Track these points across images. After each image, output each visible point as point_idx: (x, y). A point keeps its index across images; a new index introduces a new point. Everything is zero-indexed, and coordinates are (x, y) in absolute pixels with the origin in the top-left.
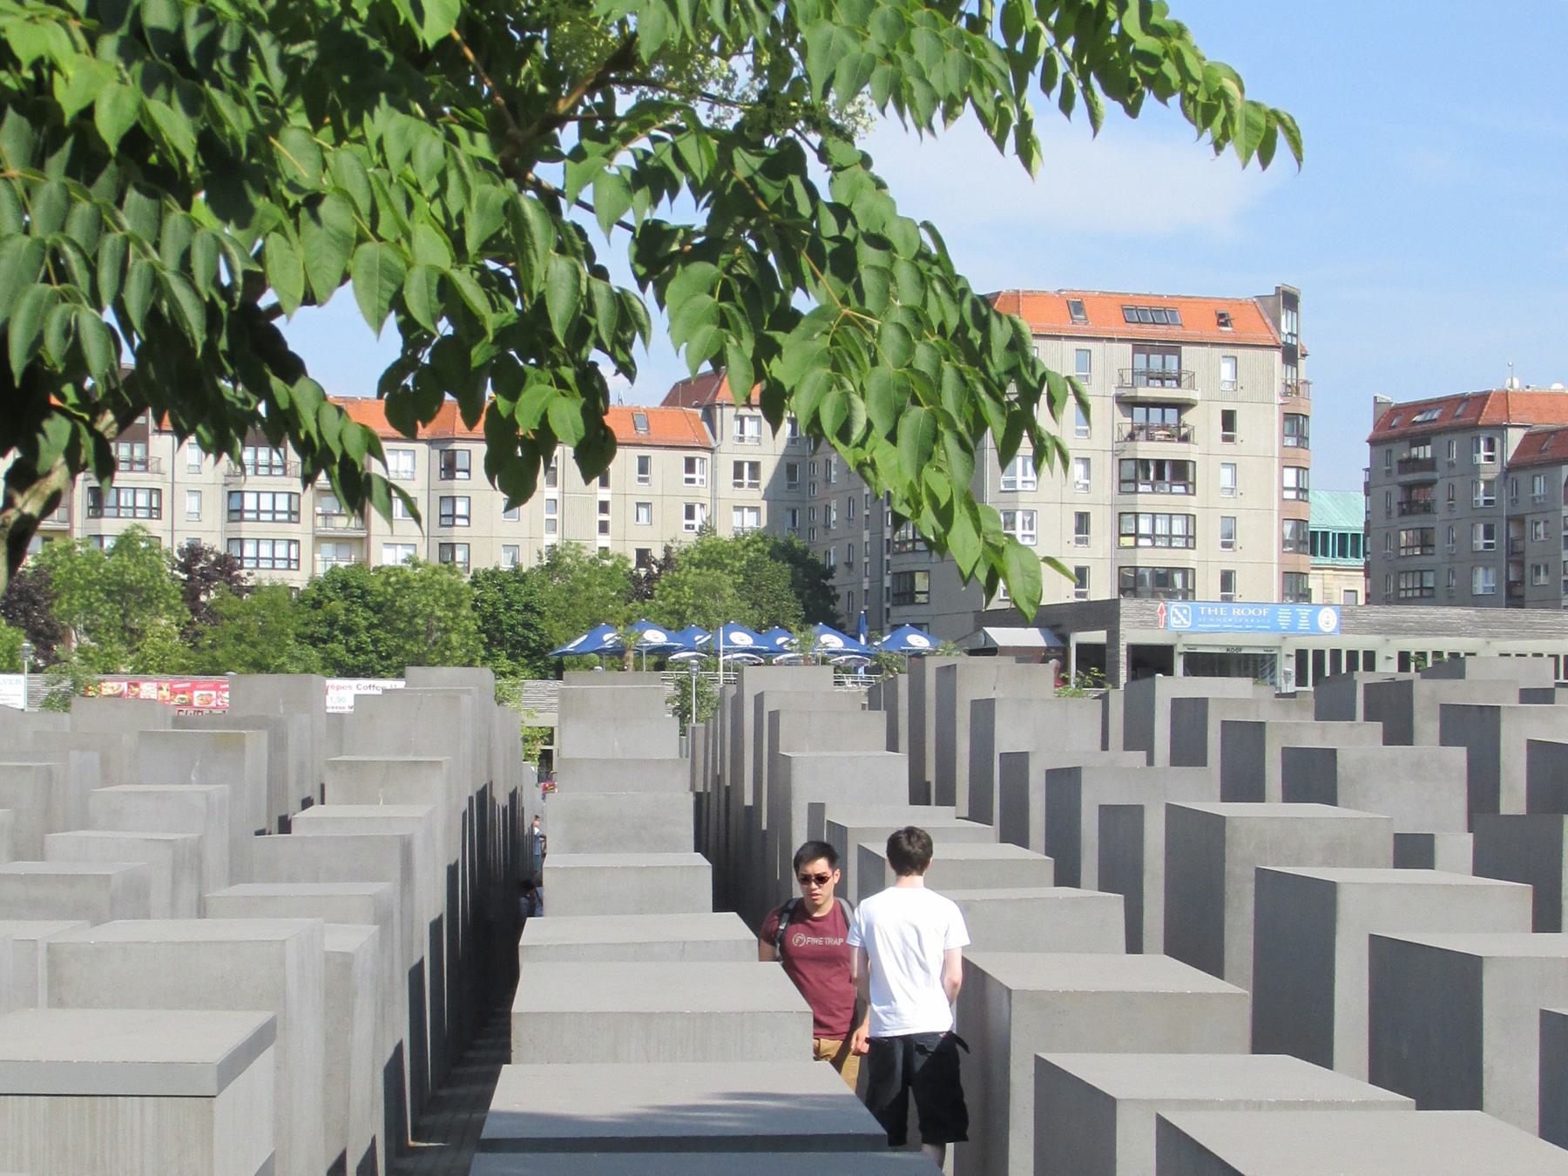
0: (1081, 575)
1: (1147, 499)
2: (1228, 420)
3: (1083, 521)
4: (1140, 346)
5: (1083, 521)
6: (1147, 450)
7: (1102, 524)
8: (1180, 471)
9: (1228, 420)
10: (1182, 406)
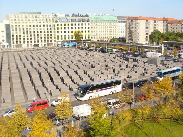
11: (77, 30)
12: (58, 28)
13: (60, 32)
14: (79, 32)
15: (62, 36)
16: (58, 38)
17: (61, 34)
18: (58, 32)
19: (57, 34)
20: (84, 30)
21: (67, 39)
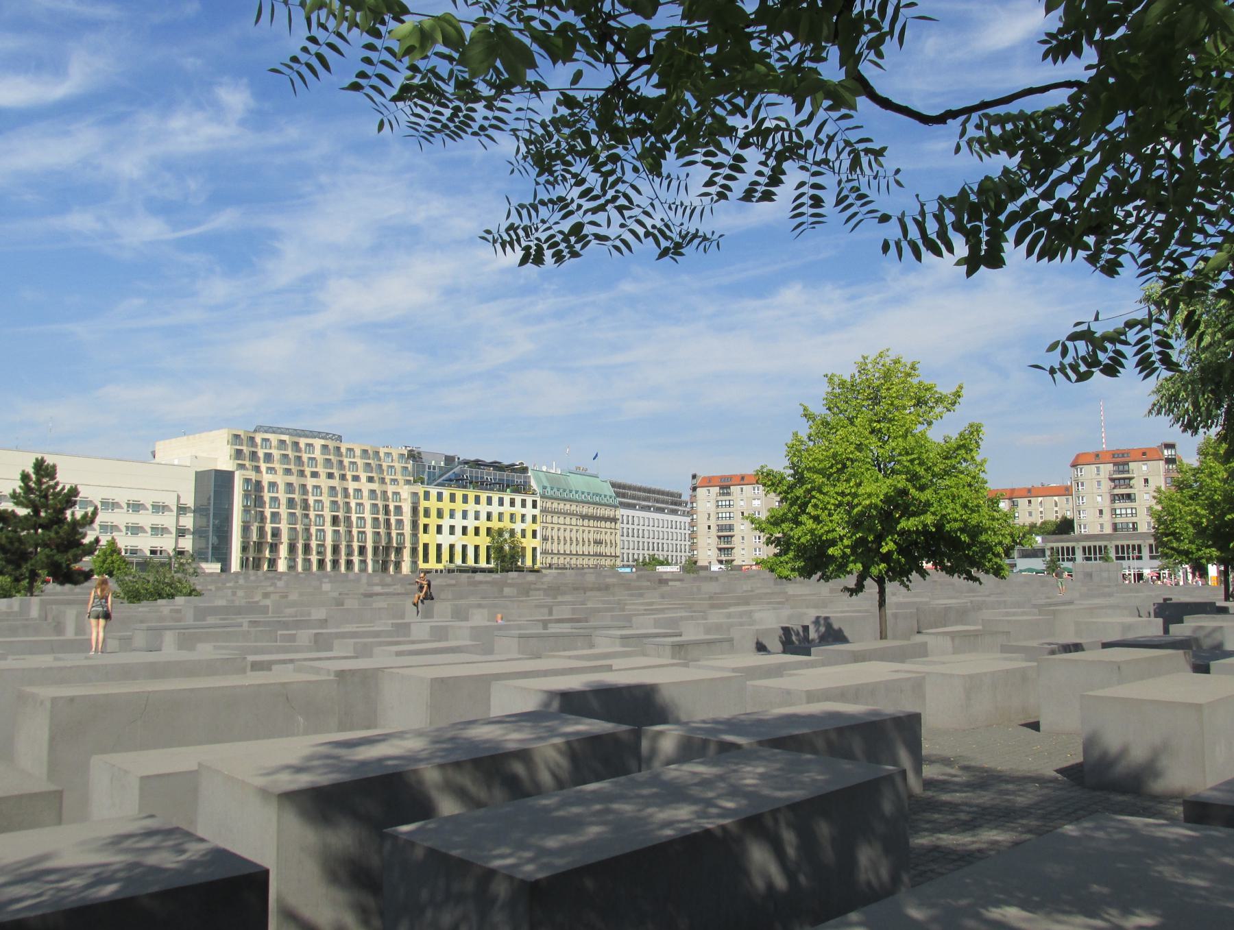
0: (1102, 525)
1: (1117, 505)
2: (1146, 481)
3: (1101, 512)
4: (1115, 464)
5: (1101, 512)
6: (1117, 491)
7: (1107, 512)
8: (1129, 497)
9: (1146, 481)
10: (1130, 479)
11: (495, 524)
12: (427, 513)
13: (433, 529)
14: (500, 532)
15: (439, 547)
16: (426, 560)
17: (440, 539)
18: (426, 527)
19: (423, 538)
20: (518, 527)
21: (458, 560)
